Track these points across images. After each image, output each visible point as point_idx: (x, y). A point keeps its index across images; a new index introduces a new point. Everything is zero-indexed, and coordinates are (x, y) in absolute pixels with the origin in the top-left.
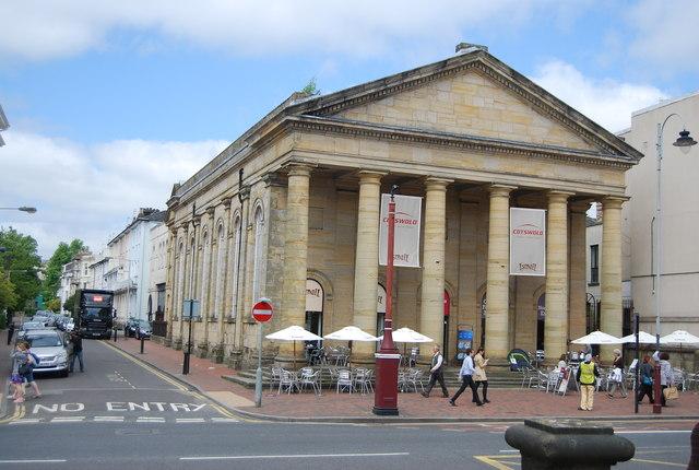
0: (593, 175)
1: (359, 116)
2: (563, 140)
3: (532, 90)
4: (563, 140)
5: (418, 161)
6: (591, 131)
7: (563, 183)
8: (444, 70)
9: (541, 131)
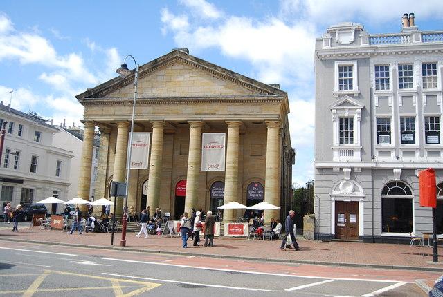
0: (256, 108)
1: (115, 96)
2: (231, 91)
3: (208, 66)
4: (231, 91)
5: (146, 114)
6: (251, 83)
7: (233, 116)
8: (156, 65)
9: (218, 89)
